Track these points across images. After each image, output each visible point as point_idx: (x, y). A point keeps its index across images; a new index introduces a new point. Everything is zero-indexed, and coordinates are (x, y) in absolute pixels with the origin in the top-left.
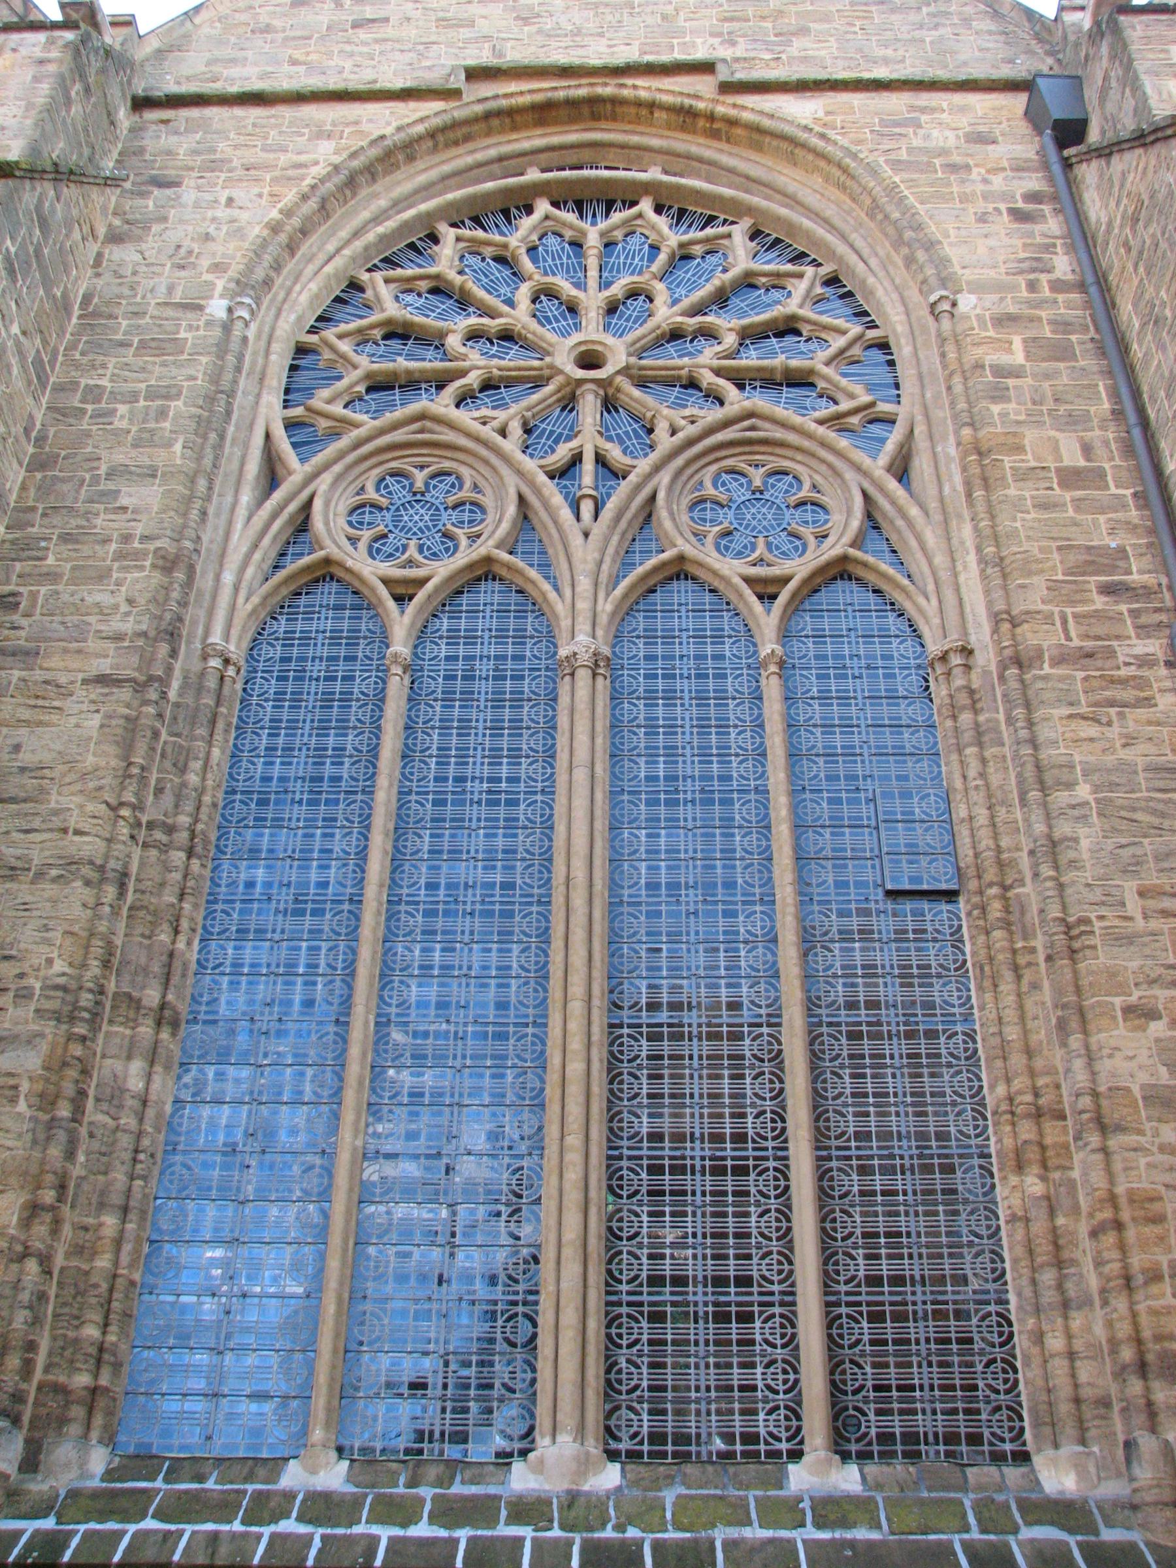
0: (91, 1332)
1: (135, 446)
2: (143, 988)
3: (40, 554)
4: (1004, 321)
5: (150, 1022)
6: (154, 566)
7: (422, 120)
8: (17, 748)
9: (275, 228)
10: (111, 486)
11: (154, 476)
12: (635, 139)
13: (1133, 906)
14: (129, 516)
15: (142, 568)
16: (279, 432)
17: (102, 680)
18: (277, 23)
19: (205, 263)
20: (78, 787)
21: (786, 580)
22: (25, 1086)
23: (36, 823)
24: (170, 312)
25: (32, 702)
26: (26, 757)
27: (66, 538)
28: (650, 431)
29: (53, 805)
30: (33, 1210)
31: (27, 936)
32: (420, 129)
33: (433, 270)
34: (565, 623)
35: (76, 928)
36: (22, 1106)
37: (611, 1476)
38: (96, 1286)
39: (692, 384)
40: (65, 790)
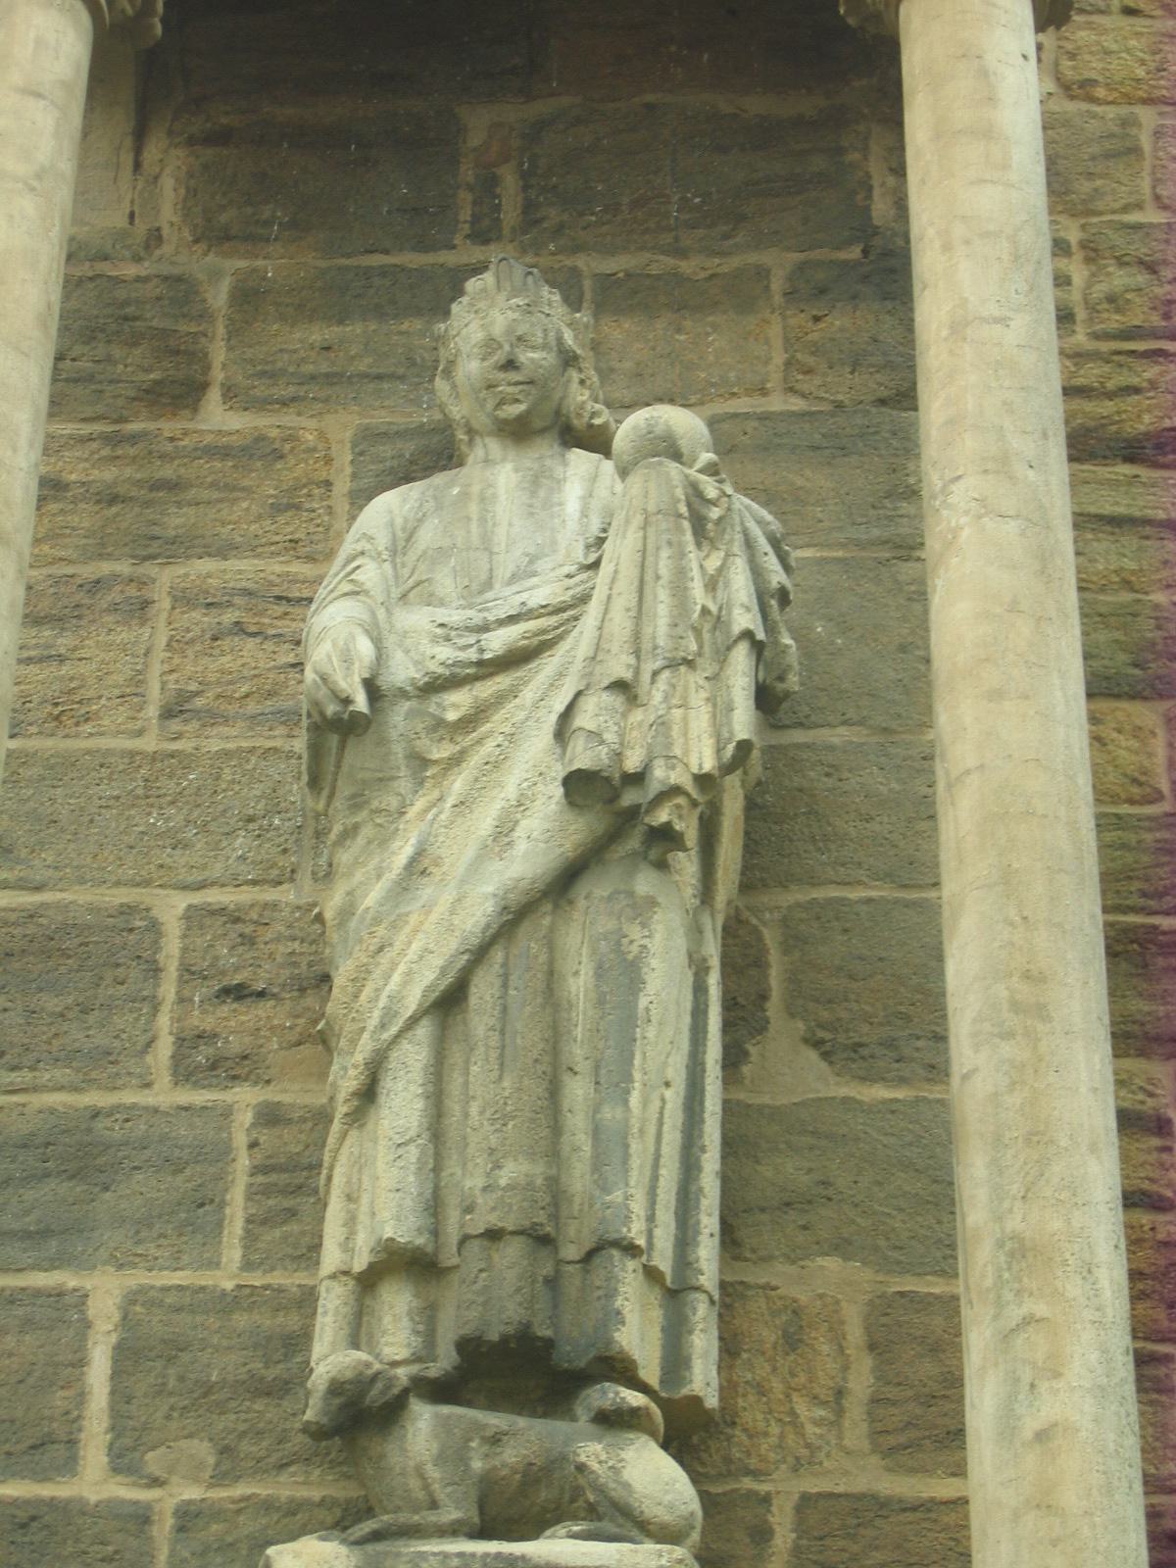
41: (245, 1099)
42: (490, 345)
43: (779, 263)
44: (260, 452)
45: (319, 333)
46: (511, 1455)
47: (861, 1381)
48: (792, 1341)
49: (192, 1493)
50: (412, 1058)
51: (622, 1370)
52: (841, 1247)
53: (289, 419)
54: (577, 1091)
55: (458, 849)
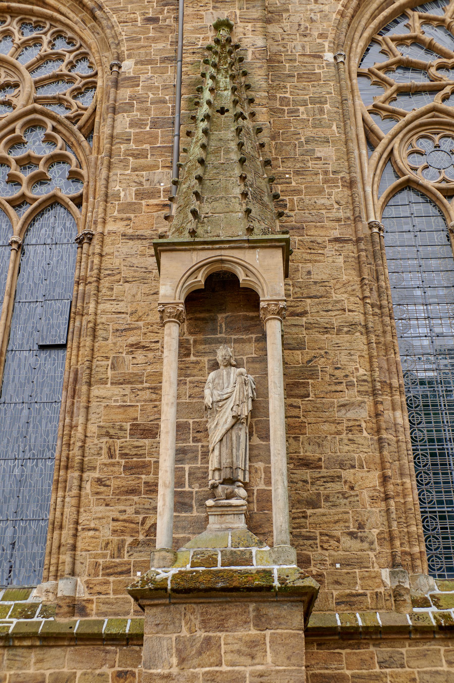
0: (414, 528)
1: (314, 127)
2: (390, 378)
3: (287, 181)
5: (398, 393)
6: (343, 186)
8: (309, 273)
9: (342, 15)
10: (309, 147)
11: (329, 142)
14: (323, 162)
15: (338, 187)
17: (337, 240)
19: (316, 34)
20: (343, 290)
22: (364, 425)
23: (330, 307)
24: (306, 59)
25: (309, 251)
26: (315, 277)
27: (297, 173)
29: (334, 298)
30: (385, 479)
31: (343, 358)
33: (413, 34)
35: (363, 354)
36: (365, 434)
38: (410, 509)
40: (338, 291)
41: (200, 444)
42: (222, 356)
43: (254, 336)
44: (197, 363)
45: (203, 347)
46: (229, 491)
47: (263, 476)
48: (256, 472)
49: (197, 489)
50: (217, 447)
51: (240, 481)
52: (261, 461)
53: (200, 358)
54: (234, 450)
55: (221, 423)
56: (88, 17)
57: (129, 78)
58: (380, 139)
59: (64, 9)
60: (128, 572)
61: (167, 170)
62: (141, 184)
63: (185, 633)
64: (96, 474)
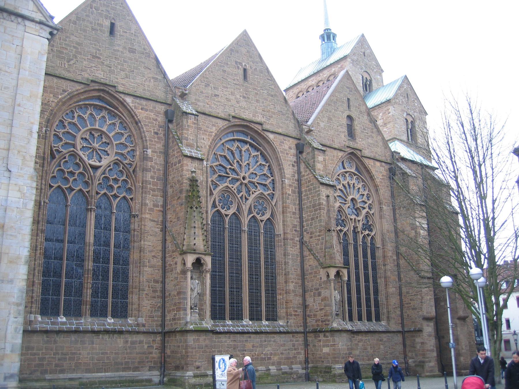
4: (290, 185)
7: (226, 125)
9: (210, 147)
12: (249, 132)
13: (293, 271)
16: (211, 185)
18: (203, 91)
21: (264, 220)
28: (249, 191)
32: (225, 127)
34: (243, 224)
37: (251, 323)
39: (254, 184)
43: (198, 271)
56: (133, 121)
57: (150, 158)
58: (213, 194)
59: (125, 114)
60: (154, 317)
61: (161, 198)
62: (154, 201)
63: (194, 337)
64: (146, 292)
